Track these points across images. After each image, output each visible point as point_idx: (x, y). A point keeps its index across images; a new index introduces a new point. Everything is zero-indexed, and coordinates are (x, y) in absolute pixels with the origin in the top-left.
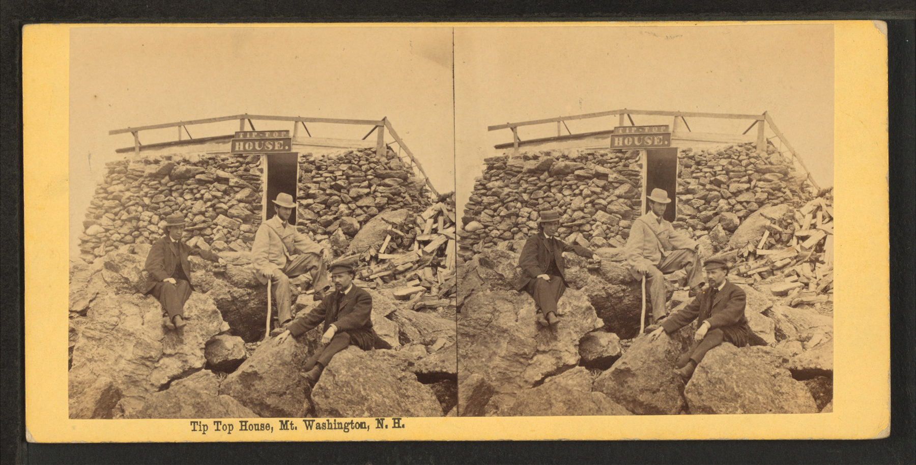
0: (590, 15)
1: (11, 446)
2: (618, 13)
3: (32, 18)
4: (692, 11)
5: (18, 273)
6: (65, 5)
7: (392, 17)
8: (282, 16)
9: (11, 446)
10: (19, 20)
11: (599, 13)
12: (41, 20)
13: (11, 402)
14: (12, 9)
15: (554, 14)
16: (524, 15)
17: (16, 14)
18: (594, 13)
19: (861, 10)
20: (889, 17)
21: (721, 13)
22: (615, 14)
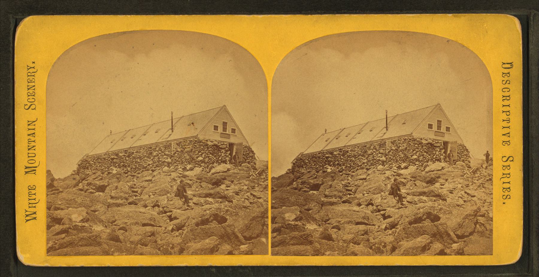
0: (340, 12)
1: (8, 259)
2: (356, 10)
3: (19, 14)
4: (399, 10)
5: (12, 160)
6: (39, 6)
7: (227, 13)
8: (164, 13)
9: (8, 259)
10: (12, 15)
11: (346, 11)
12: (25, 14)
13: (8, 234)
14: (8, 9)
15: (319, 11)
16: (303, 12)
17: (10, 11)
18: (343, 11)
19: (496, 9)
20: (514, 14)
21: (415, 11)
22: (355, 11)
